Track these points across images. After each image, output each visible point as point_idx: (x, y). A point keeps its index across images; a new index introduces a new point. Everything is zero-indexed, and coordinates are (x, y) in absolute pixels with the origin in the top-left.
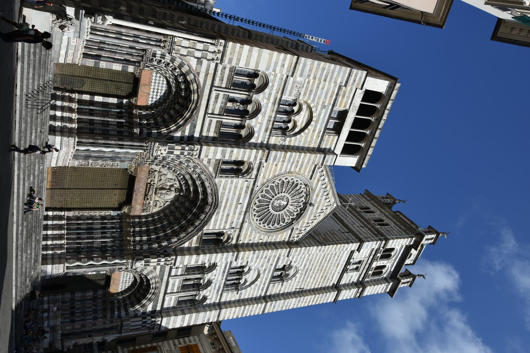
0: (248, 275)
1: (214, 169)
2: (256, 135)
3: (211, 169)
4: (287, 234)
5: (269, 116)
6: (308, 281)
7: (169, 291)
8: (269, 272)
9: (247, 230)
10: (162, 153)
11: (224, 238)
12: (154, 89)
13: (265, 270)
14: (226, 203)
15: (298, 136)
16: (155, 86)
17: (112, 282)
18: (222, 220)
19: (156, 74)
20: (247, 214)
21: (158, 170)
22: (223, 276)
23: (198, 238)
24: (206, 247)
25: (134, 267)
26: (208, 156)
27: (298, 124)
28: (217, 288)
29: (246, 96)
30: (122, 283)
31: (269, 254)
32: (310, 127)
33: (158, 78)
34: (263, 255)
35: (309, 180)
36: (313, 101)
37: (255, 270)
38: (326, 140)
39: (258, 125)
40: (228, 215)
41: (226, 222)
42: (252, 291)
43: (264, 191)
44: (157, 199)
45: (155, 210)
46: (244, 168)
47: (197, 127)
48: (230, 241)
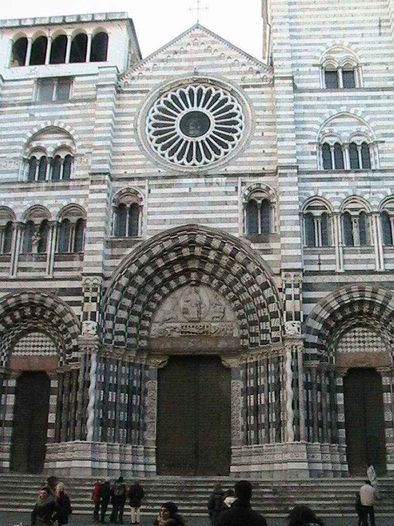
0: (343, 135)
1: (128, 247)
2: (73, 200)
3: (130, 250)
4: (252, 93)
5: (47, 190)
6: (362, 18)
7: (371, 267)
8: (336, 98)
9: (242, 164)
10: (93, 328)
11: (259, 198)
12: (33, 351)
13: (330, 107)
14: (189, 212)
15: (75, 137)
16: (29, 351)
17: (360, 365)
18: (220, 212)
19: (14, 351)
20: (209, 173)
21: (157, 325)
22: (340, 179)
23: (255, 242)
24: (274, 223)
25: (300, 336)
26: (98, 262)
27: (59, 144)
28: (368, 183)
29: (19, 232)
30: (364, 347)
31: (285, 113)
32: (61, 126)
33: (20, 349)
34: (286, 123)
35: (149, 93)
36: (23, 136)
37: (332, 125)
38: (80, 94)
39: (59, 202)
40: (212, 203)
41: (226, 203)
42: (378, 116)
43: (171, 158)
44: (209, 318)
45: (230, 316)
46: (128, 201)
47: (64, 287)
48: (262, 187)
